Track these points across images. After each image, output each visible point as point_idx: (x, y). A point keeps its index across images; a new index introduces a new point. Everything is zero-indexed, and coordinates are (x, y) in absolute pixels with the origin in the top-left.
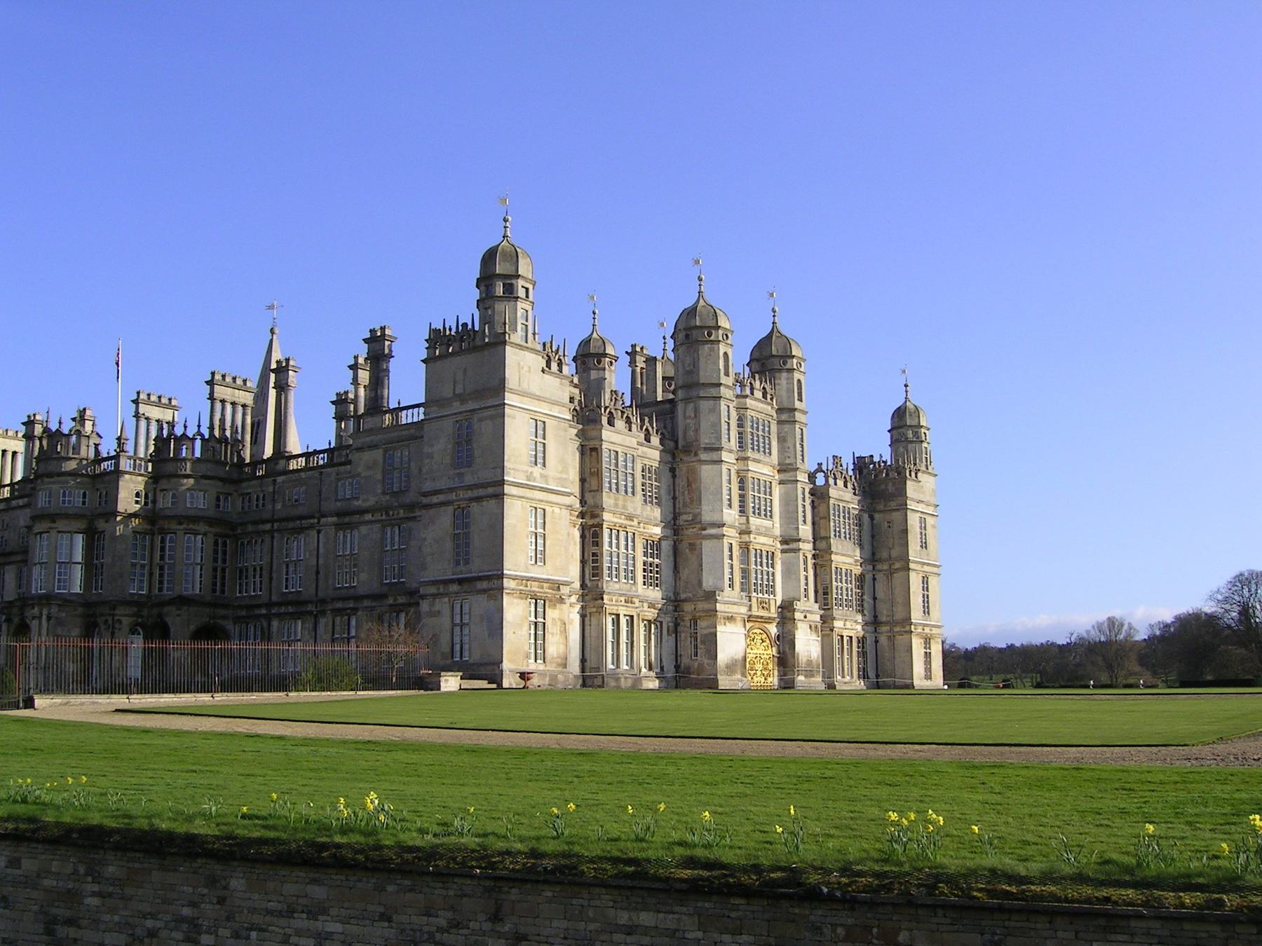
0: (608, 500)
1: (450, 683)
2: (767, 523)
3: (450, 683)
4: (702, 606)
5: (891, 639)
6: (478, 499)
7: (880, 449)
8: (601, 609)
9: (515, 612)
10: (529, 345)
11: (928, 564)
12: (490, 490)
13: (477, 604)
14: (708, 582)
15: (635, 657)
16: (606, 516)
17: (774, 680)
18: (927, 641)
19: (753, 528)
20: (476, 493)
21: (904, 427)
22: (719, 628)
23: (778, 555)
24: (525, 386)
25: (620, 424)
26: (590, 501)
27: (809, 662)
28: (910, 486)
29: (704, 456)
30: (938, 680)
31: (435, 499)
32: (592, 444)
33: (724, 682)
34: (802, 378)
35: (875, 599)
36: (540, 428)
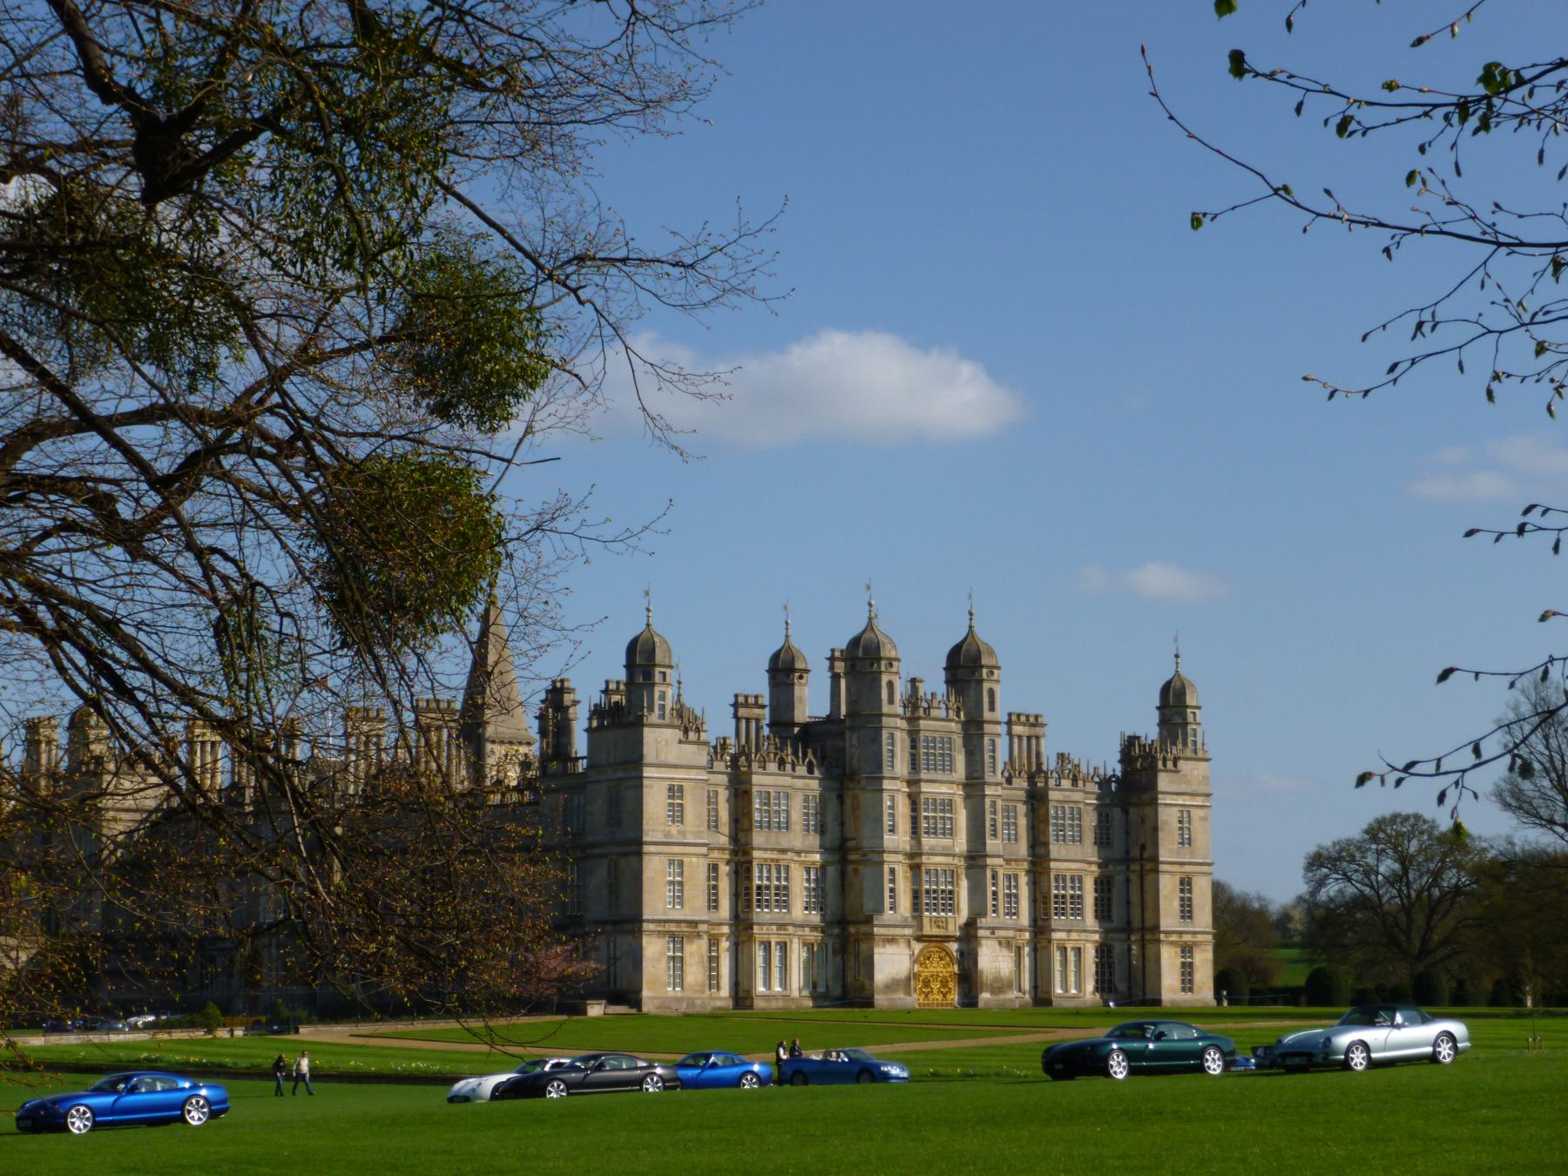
0: (758, 838)
1: (595, 1010)
2: (946, 842)
3: (595, 1010)
4: (863, 928)
5: (1143, 948)
6: (625, 855)
7: (1149, 730)
8: (751, 937)
9: (653, 949)
10: (667, 720)
11: (1190, 864)
12: (634, 848)
13: (623, 942)
14: (868, 906)
15: (785, 980)
16: (756, 854)
17: (954, 997)
18: (1187, 949)
19: (926, 848)
20: (627, 849)
21: (1173, 704)
22: (876, 950)
23: (962, 872)
24: (663, 759)
25: (772, 767)
26: (743, 840)
27: (997, 979)
28: (1164, 782)
29: (863, 783)
30: (1204, 991)
31: (597, 851)
32: (743, 787)
33: (880, 999)
34: (993, 686)
35: (1128, 902)
36: (675, 791)
